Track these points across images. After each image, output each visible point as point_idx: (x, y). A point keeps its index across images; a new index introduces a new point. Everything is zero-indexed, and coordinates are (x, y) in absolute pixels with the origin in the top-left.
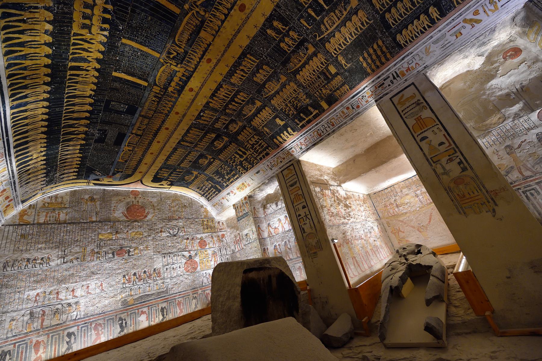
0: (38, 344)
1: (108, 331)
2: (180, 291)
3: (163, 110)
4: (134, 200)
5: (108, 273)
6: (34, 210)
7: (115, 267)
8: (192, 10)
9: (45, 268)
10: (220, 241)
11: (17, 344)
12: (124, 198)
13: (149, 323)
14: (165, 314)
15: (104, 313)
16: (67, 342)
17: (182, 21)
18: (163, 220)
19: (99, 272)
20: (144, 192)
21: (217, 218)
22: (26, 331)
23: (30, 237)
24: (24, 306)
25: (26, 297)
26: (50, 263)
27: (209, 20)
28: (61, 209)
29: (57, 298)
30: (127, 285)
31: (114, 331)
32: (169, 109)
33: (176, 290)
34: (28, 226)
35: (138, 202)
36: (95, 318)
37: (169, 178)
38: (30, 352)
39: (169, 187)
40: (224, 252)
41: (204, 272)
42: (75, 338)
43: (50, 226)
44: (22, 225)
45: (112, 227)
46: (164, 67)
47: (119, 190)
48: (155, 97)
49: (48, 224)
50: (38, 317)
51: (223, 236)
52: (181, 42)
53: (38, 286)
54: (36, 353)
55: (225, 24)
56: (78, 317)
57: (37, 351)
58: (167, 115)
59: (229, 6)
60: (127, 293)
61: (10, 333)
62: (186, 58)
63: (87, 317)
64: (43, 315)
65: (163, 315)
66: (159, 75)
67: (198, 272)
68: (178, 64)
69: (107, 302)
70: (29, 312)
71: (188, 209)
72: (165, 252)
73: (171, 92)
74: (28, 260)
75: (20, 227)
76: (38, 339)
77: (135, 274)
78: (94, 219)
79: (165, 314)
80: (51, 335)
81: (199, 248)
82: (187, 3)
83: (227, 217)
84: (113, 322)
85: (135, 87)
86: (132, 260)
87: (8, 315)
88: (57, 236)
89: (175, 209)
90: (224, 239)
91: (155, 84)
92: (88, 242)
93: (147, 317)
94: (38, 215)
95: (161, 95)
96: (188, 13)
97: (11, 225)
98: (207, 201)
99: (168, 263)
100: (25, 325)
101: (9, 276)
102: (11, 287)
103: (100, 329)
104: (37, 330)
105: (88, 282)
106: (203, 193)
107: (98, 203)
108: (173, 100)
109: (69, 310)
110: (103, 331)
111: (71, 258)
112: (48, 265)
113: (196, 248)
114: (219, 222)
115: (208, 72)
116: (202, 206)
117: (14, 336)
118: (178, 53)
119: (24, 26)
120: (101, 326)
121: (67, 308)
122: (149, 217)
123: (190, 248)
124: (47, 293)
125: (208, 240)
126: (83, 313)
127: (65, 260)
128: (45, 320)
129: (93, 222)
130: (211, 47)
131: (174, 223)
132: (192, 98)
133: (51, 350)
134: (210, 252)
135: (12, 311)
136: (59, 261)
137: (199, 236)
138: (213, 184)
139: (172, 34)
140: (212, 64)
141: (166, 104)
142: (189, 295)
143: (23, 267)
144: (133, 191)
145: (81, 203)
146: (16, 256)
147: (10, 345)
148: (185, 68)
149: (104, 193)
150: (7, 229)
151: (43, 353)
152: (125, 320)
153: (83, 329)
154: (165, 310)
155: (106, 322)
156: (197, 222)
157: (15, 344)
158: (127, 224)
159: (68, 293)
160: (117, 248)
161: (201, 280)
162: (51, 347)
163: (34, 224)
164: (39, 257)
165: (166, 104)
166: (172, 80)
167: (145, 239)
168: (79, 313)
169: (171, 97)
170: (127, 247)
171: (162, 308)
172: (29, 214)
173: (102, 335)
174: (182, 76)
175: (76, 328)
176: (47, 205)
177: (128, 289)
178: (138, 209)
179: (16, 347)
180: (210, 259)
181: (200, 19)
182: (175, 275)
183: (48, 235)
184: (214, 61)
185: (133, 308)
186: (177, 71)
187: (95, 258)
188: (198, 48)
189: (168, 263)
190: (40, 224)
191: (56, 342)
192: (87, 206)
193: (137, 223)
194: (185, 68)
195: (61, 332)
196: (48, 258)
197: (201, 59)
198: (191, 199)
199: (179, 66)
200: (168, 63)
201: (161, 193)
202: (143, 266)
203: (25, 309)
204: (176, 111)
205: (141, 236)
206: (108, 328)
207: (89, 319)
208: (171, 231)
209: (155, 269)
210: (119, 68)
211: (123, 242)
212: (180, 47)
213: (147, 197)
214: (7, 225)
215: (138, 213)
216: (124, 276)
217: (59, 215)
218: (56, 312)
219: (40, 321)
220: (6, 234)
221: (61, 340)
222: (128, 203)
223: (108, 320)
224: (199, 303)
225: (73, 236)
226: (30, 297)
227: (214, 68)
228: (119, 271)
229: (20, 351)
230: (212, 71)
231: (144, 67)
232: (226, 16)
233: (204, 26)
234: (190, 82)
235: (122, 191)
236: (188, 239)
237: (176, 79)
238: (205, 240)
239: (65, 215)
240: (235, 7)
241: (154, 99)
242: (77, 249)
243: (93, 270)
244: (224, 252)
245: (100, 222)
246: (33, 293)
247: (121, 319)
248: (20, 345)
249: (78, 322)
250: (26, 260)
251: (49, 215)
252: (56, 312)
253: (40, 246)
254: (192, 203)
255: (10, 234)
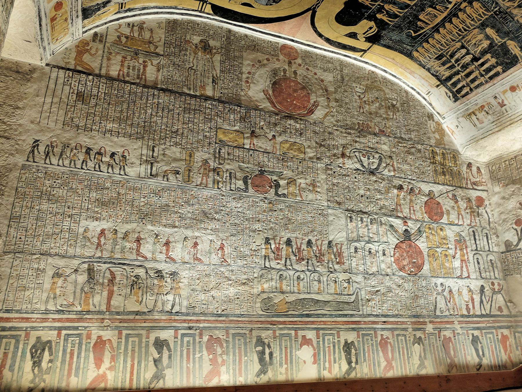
0: (100, 344)
1: (234, 361)
2: (386, 312)
4: (287, 67)
5: (235, 225)
6: (101, 46)
7: (249, 214)
9: (118, 178)
10: (474, 213)
11: (64, 332)
12: (268, 60)
13: (319, 371)
14: (354, 360)
15: (227, 316)
16: (155, 361)
18: (348, 128)
19: (217, 216)
20: (307, 55)
21: (468, 154)
22: (79, 308)
23: (93, 102)
24: (78, 251)
25: (81, 230)
26: (127, 170)
28: (148, 54)
29: (138, 253)
30: (273, 264)
31: (246, 366)
33: (374, 307)
34: (91, 77)
35: (295, 73)
36: (209, 321)
37: (380, 10)
38: (87, 358)
39: (365, 45)
40: (482, 243)
41: (440, 281)
42: (170, 357)
43: (128, 87)
44: (80, 72)
45: (243, 119)
47: (259, 39)
49: (125, 82)
50: (103, 284)
51: (480, 201)
53: (104, 214)
54: (98, 366)
56: (176, 309)
57: (99, 362)
60: (273, 283)
61: (51, 303)
63: (194, 314)
64: (112, 281)
65: (349, 363)
67: (426, 278)
69: (232, 291)
70: (86, 266)
71: (399, 116)
72: (351, 206)
74: (88, 150)
75: (77, 76)
76: (101, 333)
77: (289, 242)
78: (209, 92)
79: (354, 360)
80: (124, 332)
81: (427, 219)
83: (495, 155)
84: (245, 344)
86: (282, 206)
87: (50, 260)
88: (140, 113)
89: (373, 108)
90: (481, 210)
92: (198, 142)
93: (314, 355)
94: (109, 59)
97: (63, 68)
98: (450, 103)
99: (359, 236)
100: (78, 294)
101: (55, 176)
102: (57, 201)
103: (219, 351)
104: (100, 312)
105: (197, 234)
106: (447, 74)
107: (217, 58)
109: (160, 287)
110: (225, 357)
111: (165, 168)
112: (122, 173)
113: (419, 216)
114: (469, 165)
116: (430, 117)
117: (59, 312)
120: (222, 346)
121: (156, 282)
122: (319, 114)
123: (406, 212)
124: (120, 235)
125: (446, 204)
126: (185, 303)
127: (154, 169)
128: (115, 295)
129: (207, 98)
131: (371, 141)
133: (125, 367)
134: (450, 233)
135: (56, 255)
136: (143, 167)
137: (426, 188)
138: (498, 39)
142: (405, 329)
143: (79, 164)
144: (284, 46)
145: (186, 50)
146: (67, 135)
147: (51, 328)
149: (228, 38)
150: (54, 75)
151: (110, 369)
152: (269, 346)
153: (186, 339)
154: (353, 351)
155: (231, 339)
156: (419, 151)
157: (60, 329)
158: (273, 120)
159: (158, 247)
160: (253, 171)
161: (432, 298)
162: (125, 361)
163: (99, 76)
164: (108, 149)
167: (310, 164)
168: (177, 300)
170: (272, 173)
171: (346, 342)
172: (93, 51)
173: (223, 369)
175: (172, 332)
176: (124, 40)
177: (275, 275)
178: (295, 91)
179: (62, 338)
180: (451, 252)
182: (374, 269)
183: (125, 106)
185: (284, 323)
187: (210, 180)
189: (359, 236)
190: (111, 79)
191: (133, 351)
192: (198, 61)
193: (292, 122)
195: (144, 332)
196: (123, 156)
198: (406, 92)
201: (341, 63)
202: (306, 229)
203: (80, 257)
205: (302, 156)
206: (234, 354)
207: (198, 321)
208: (365, 160)
209: (330, 242)
211: (266, 160)
213: (315, 67)
214: (54, 67)
215: (295, 98)
216: (267, 241)
217: (145, 67)
218: (135, 283)
219: (105, 294)
220: (52, 86)
221: (143, 350)
222: (275, 72)
223: (234, 335)
224: (428, 356)
225: (170, 122)
226: (89, 235)
228: (257, 226)
229: (69, 350)
235: (264, 41)
236: (400, 188)
238: (440, 201)
239: (155, 69)
242: (175, 152)
243: (205, 207)
244: (482, 243)
245: (220, 101)
246: (95, 227)
247: (260, 342)
248: (68, 335)
249: (175, 321)
250: (84, 150)
251: (126, 64)
252: (135, 283)
253: (109, 126)
254: (406, 104)
255: (59, 87)
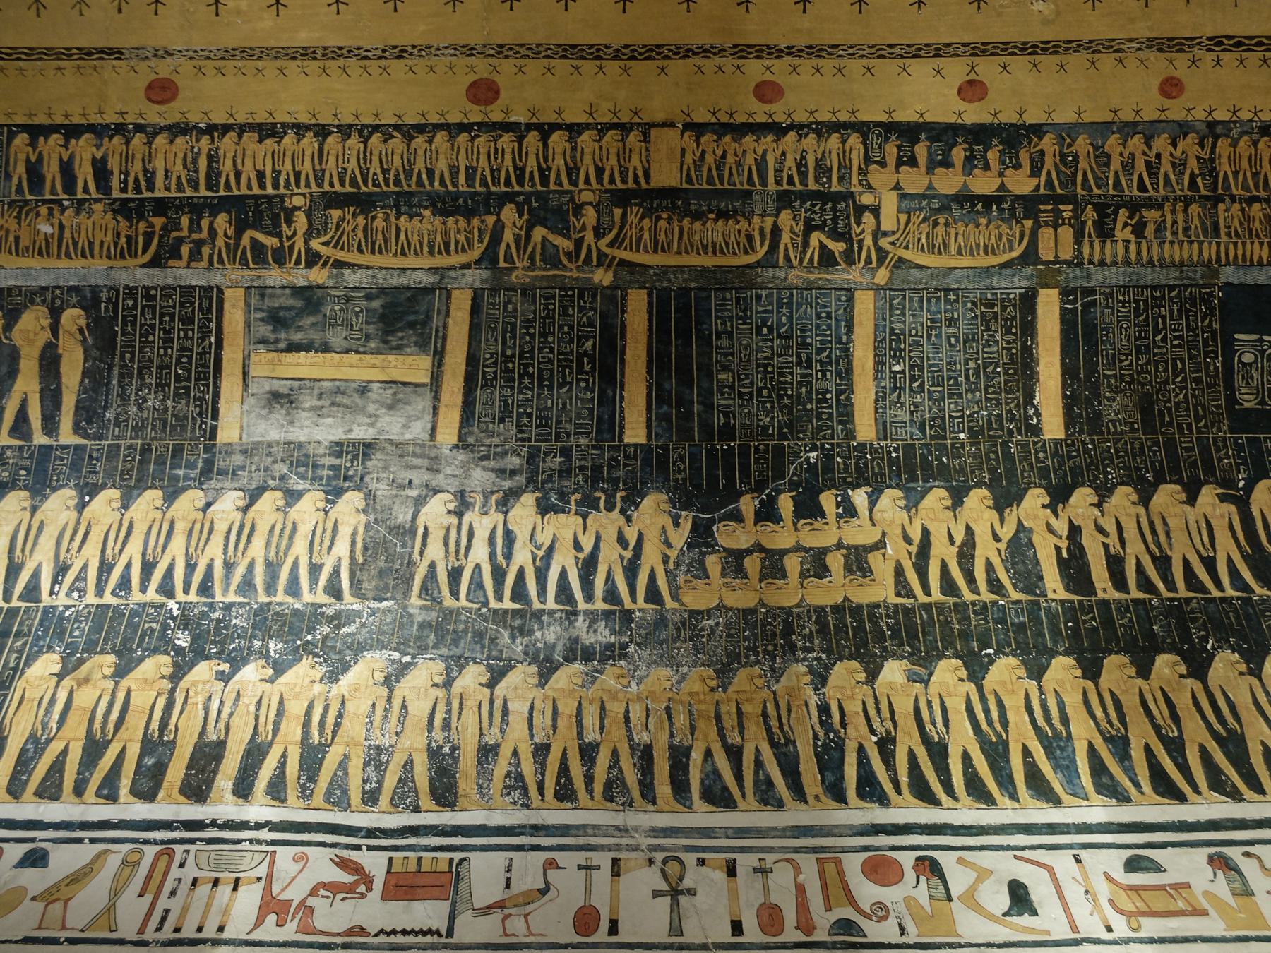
3: (1179, 166)
8: (601, 255)
17: (665, 271)
27: (600, 181)
32: (1161, 143)
46: (907, 255)
48: (1104, 232)
52: (749, 237)
55: (575, 116)
58: (1213, 130)
59: (506, 141)
62: (812, 186)
66: (966, 261)
68: (861, 210)
73: (1035, 172)
82: (590, 279)
85: (1090, 330)
91: (1031, 256)
95: (1078, 212)
96: (623, 263)
108: (1082, 145)
115: (828, 64)
118: (809, 228)
119: (908, 740)
130: (702, 116)
132: (1019, 63)
139: (740, 283)
140: (779, 69)
141: (1128, 166)
148: (863, 173)
165: (1128, 166)
166: (967, 200)
169: (1068, 161)
174: (913, 162)
181: (618, 212)
184: (755, 69)
186: (903, 196)
188: (739, 164)
194: (863, 173)
197: (779, 130)
199: (867, 199)
200: (879, 250)
204: (1158, 100)
210: (1012, 419)
212: (776, 232)
227: (790, 51)
230: (812, 51)
231: (963, 327)
232: (545, 131)
233: (631, 185)
234: (929, 118)
237: (948, 183)
240: (496, 116)
241: (1123, 234)
